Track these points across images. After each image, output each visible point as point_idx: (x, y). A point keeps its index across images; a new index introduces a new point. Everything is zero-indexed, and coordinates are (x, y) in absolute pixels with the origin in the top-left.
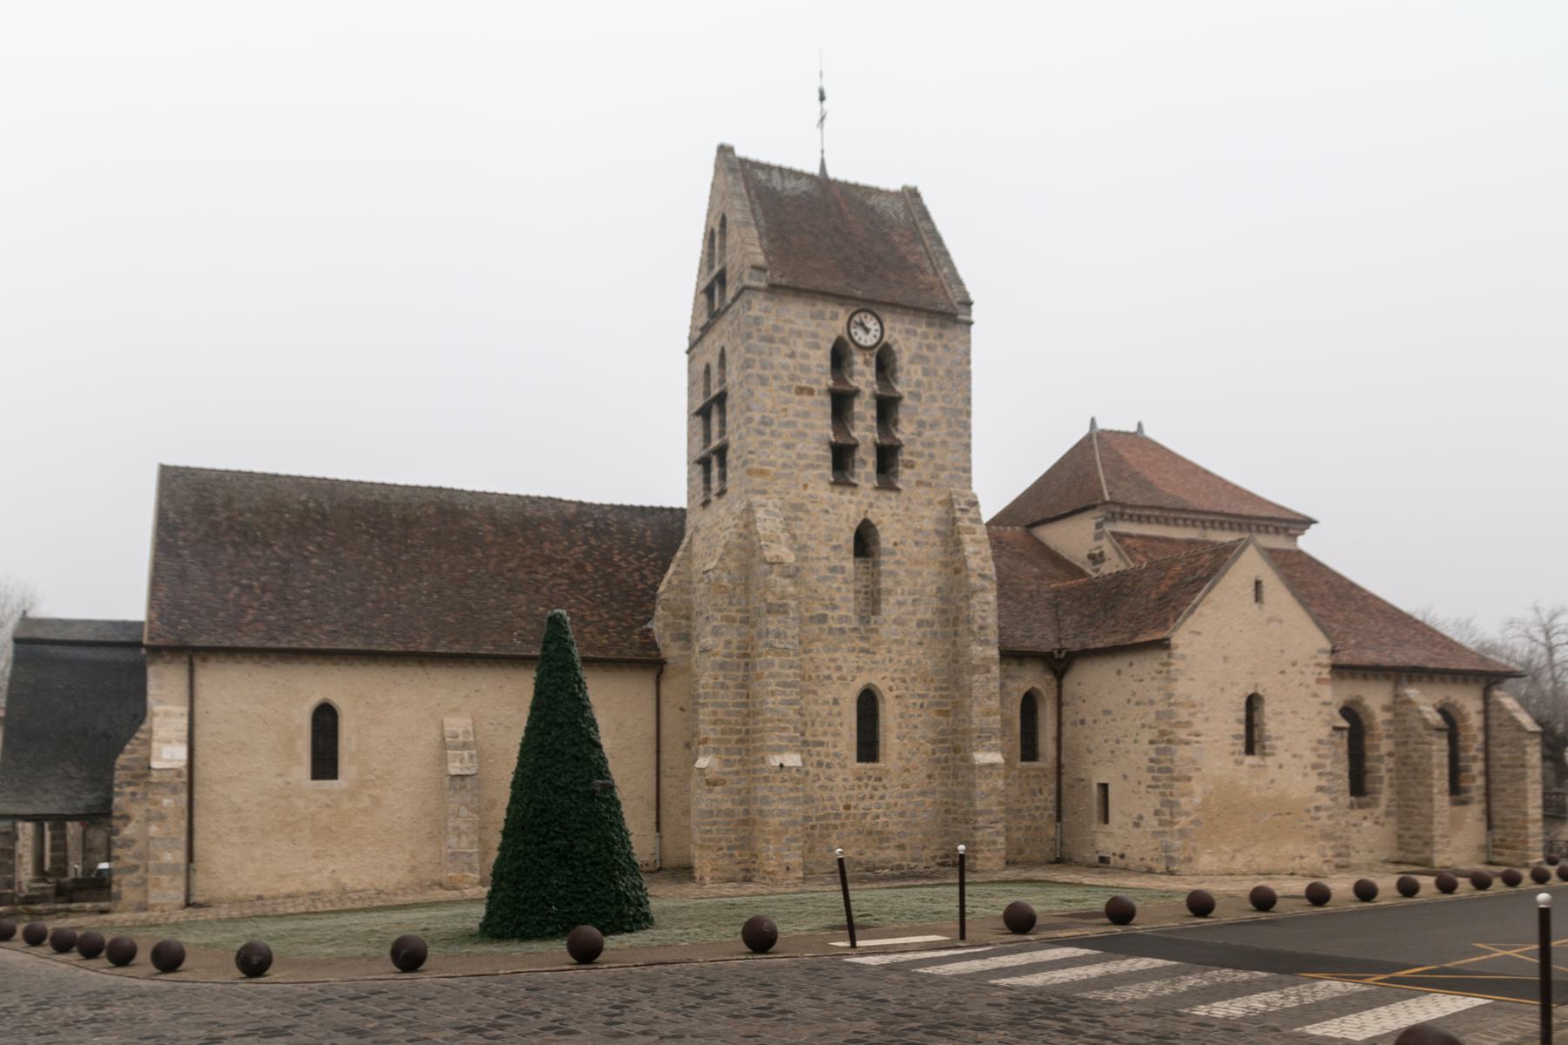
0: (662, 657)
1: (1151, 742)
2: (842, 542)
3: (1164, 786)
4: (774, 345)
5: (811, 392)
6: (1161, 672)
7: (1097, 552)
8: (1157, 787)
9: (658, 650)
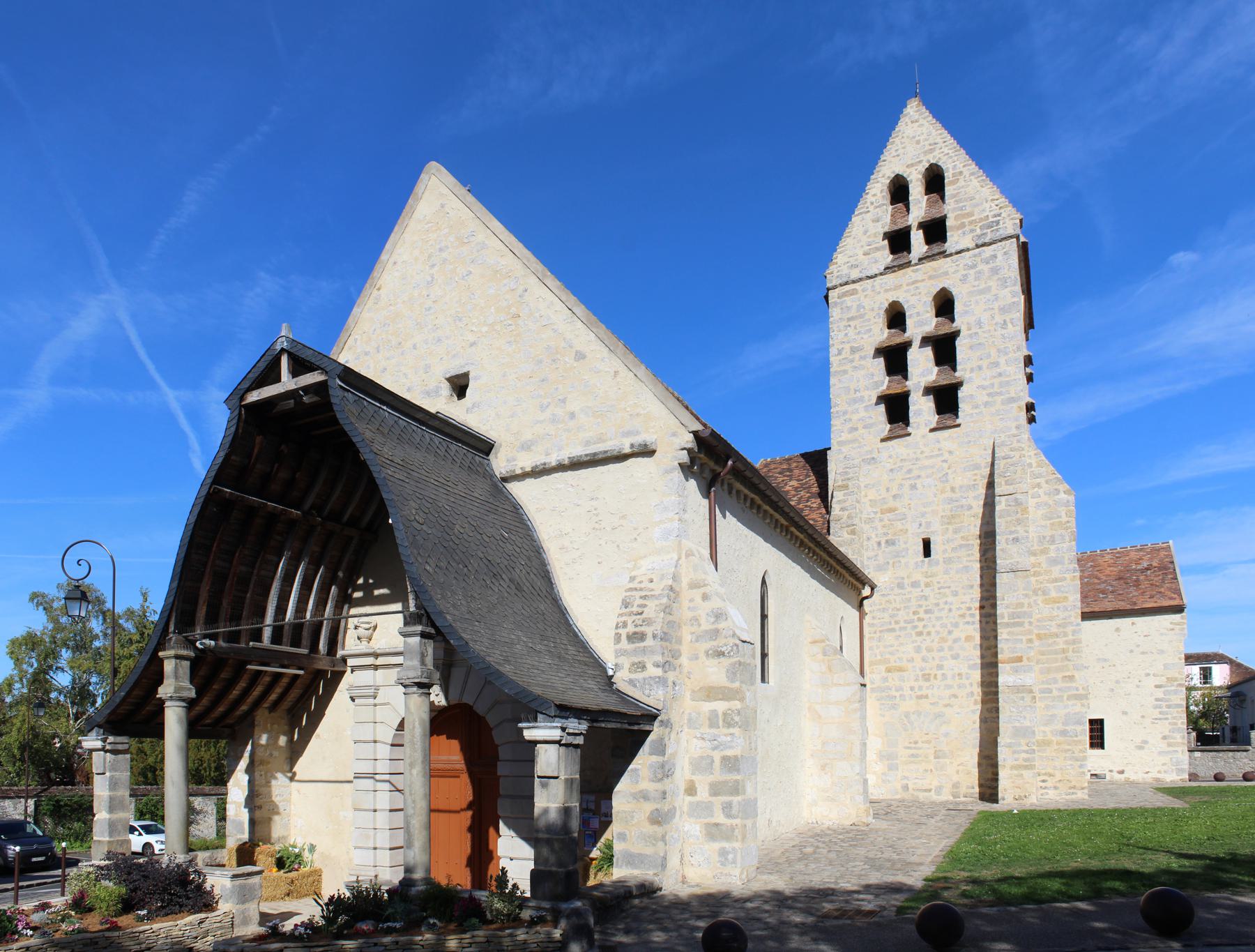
1: (1157, 686)
3: (1174, 718)
6: (1173, 629)
8: (1167, 719)
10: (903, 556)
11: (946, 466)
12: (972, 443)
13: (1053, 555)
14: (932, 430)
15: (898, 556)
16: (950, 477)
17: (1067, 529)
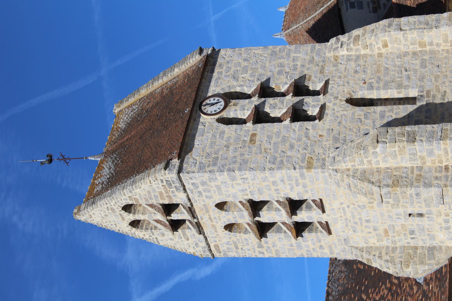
0: (447, 262)
2: (362, 113)
4: (220, 157)
5: (254, 135)
7: (371, 6)
9: (442, 268)
10: (423, 227)
11: (351, 206)
12: (334, 194)
13: (425, 153)
14: (324, 211)
15: (423, 230)
16: (360, 204)
17: (404, 147)
